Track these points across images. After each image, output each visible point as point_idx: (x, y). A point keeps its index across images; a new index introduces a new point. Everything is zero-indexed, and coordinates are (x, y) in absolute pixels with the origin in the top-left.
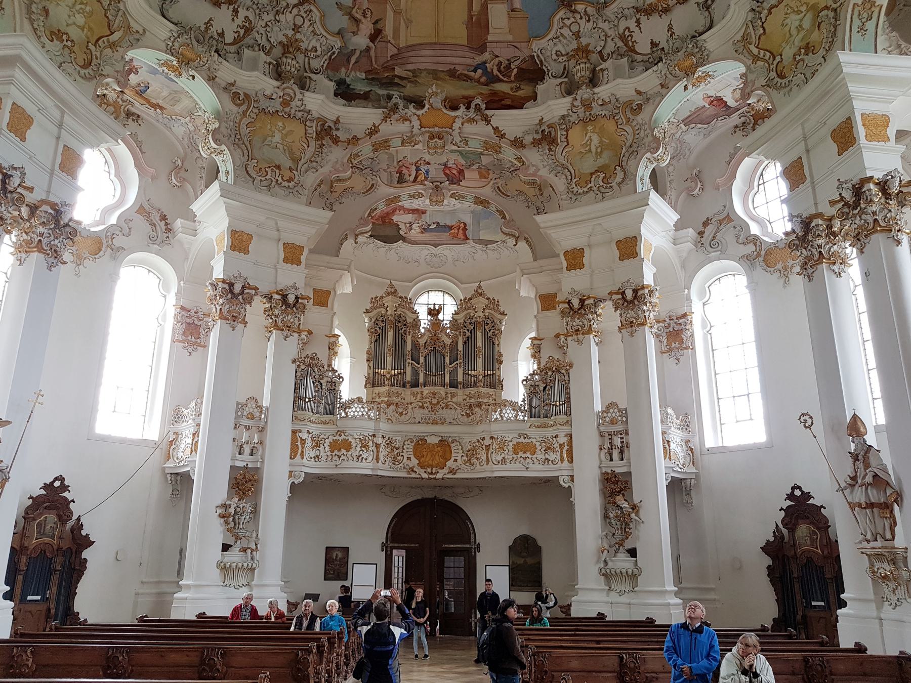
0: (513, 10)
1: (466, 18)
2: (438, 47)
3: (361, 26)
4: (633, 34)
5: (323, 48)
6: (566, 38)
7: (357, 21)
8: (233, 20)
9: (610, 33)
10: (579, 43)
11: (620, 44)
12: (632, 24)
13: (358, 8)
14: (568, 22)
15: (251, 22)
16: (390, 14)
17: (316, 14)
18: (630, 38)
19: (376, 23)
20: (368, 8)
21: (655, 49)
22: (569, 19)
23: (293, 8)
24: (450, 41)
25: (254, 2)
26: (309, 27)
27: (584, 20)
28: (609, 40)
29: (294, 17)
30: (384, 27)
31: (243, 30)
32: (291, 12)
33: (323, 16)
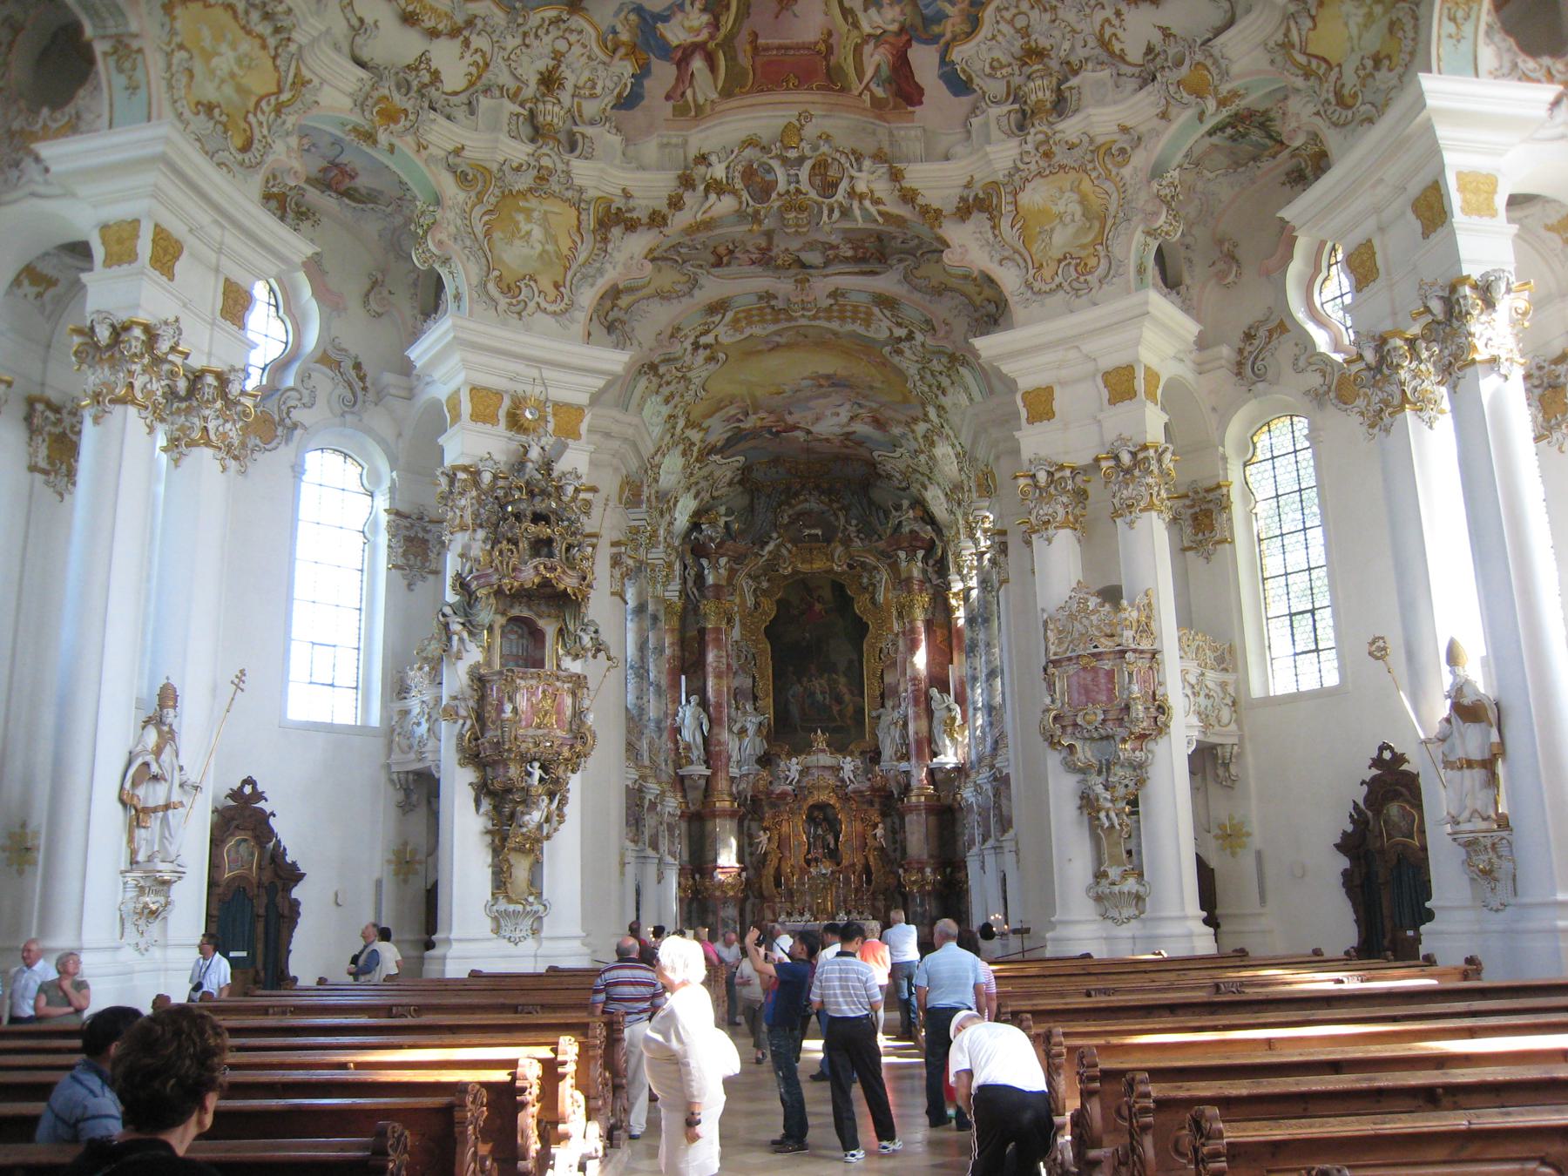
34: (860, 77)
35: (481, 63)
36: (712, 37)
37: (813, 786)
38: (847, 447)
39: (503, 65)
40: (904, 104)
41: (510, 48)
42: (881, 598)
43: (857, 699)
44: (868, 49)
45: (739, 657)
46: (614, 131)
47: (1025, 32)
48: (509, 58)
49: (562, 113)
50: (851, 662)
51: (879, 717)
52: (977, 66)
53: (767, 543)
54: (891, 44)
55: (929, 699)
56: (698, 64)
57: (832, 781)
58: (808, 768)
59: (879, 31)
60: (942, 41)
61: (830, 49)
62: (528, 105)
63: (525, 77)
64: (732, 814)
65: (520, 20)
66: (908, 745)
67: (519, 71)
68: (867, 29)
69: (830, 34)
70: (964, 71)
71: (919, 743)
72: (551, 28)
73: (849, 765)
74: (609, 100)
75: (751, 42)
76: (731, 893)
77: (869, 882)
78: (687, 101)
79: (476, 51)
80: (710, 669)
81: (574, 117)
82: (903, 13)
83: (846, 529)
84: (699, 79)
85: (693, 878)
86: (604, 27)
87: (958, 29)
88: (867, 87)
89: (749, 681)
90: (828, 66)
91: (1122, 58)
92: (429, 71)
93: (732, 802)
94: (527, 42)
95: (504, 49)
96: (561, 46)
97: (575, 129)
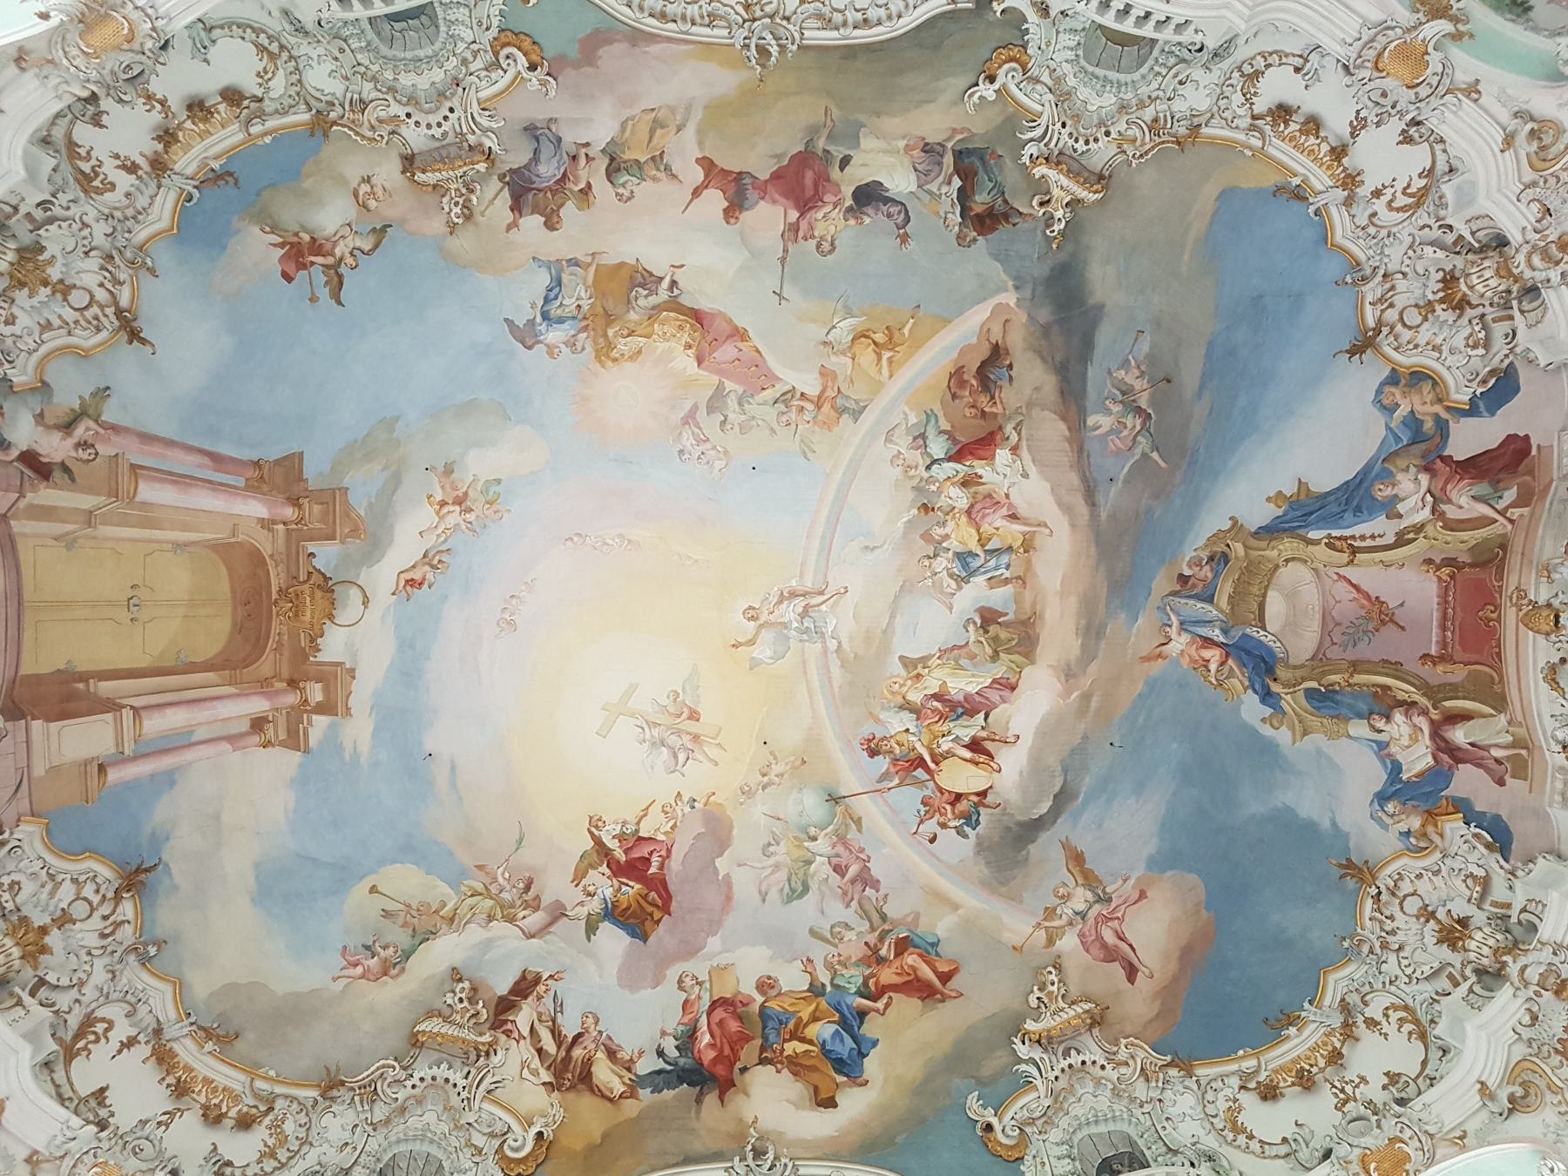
0: (102, 768)
1: (82, 666)
2: (12, 610)
3: (57, 436)
4: (103, 1040)
5: (9, 341)
6: (52, 894)
7: (68, 427)
8: (117, 157)
9: (89, 992)
10: (43, 930)
11: (74, 1021)
12: (122, 1031)
13: (97, 433)
14: (88, 891)
15: (99, 191)
16: (86, 501)
17: (85, 339)
18: (92, 1037)
19: (65, 468)
20: (97, 454)
21: (93, 1103)
22: (97, 891)
23: (110, 292)
24: (27, 635)
25: (140, 213)
26: (60, 317)
27: (100, 925)
28: (74, 993)
29: (90, 293)
30: (56, 486)
31: (87, 170)
32: (101, 285)
33: (84, 355)
34: (1487, 522)
35: (1404, 1014)
36: (1424, 712)
39: (1415, 987)
40: (1525, 462)
41: (1399, 973)
44: (1451, 512)
46: (1531, 865)
47: (1429, 307)
48: (1409, 977)
49: (1487, 930)
52: (1476, 363)
54: (1446, 483)
56: (1459, 735)
59: (1429, 498)
60: (1444, 415)
61: (1450, 562)
62: (1468, 972)
63: (1436, 965)
65: (1365, 949)
67: (1428, 972)
68: (1425, 514)
69: (1429, 561)
70: (1484, 382)
72: (1388, 913)
74: (1494, 861)
75: (1435, 664)
78: (1508, 757)
79: (1386, 1016)
81: (1501, 920)
82: (1406, 470)
84: (1480, 737)
86: (1399, 845)
87: (1429, 398)
88: (1502, 513)
90: (1472, 565)
91: (1429, 173)
92: (1357, 1086)
94: (1397, 946)
95: (1396, 977)
96: (1413, 905)
97: (1514, 920)
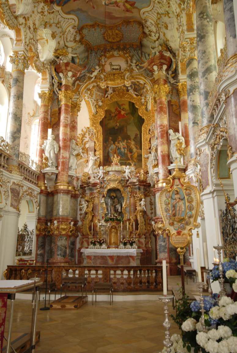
37: (110, 180)
38: (128, 10)
42: (150, 107)
43: (139, 151)
45: (89, 135)
50: (136, 135)
51: (148, 158)
53: (94, 72)
55: (168, 134)
57: (119, 177)
58: (108, 172)
64: (67, 192)
66: (157, 160)
71: (163, 156)
73: (127, 170)
76: (64, 233)
77: (137, 229)
80: (61, 124)
83: (131, 65)
85: (46, 224)
89: (94, 143)
93: (68, 186)
